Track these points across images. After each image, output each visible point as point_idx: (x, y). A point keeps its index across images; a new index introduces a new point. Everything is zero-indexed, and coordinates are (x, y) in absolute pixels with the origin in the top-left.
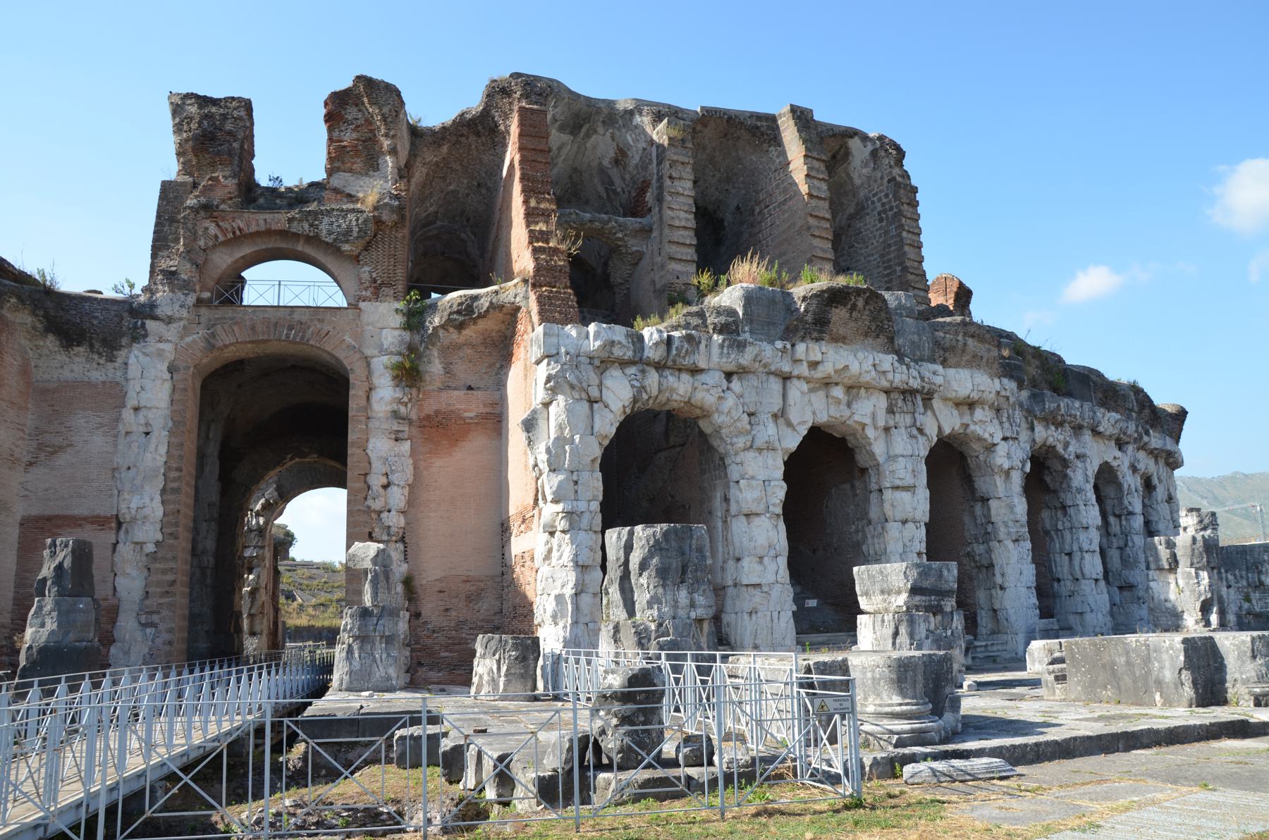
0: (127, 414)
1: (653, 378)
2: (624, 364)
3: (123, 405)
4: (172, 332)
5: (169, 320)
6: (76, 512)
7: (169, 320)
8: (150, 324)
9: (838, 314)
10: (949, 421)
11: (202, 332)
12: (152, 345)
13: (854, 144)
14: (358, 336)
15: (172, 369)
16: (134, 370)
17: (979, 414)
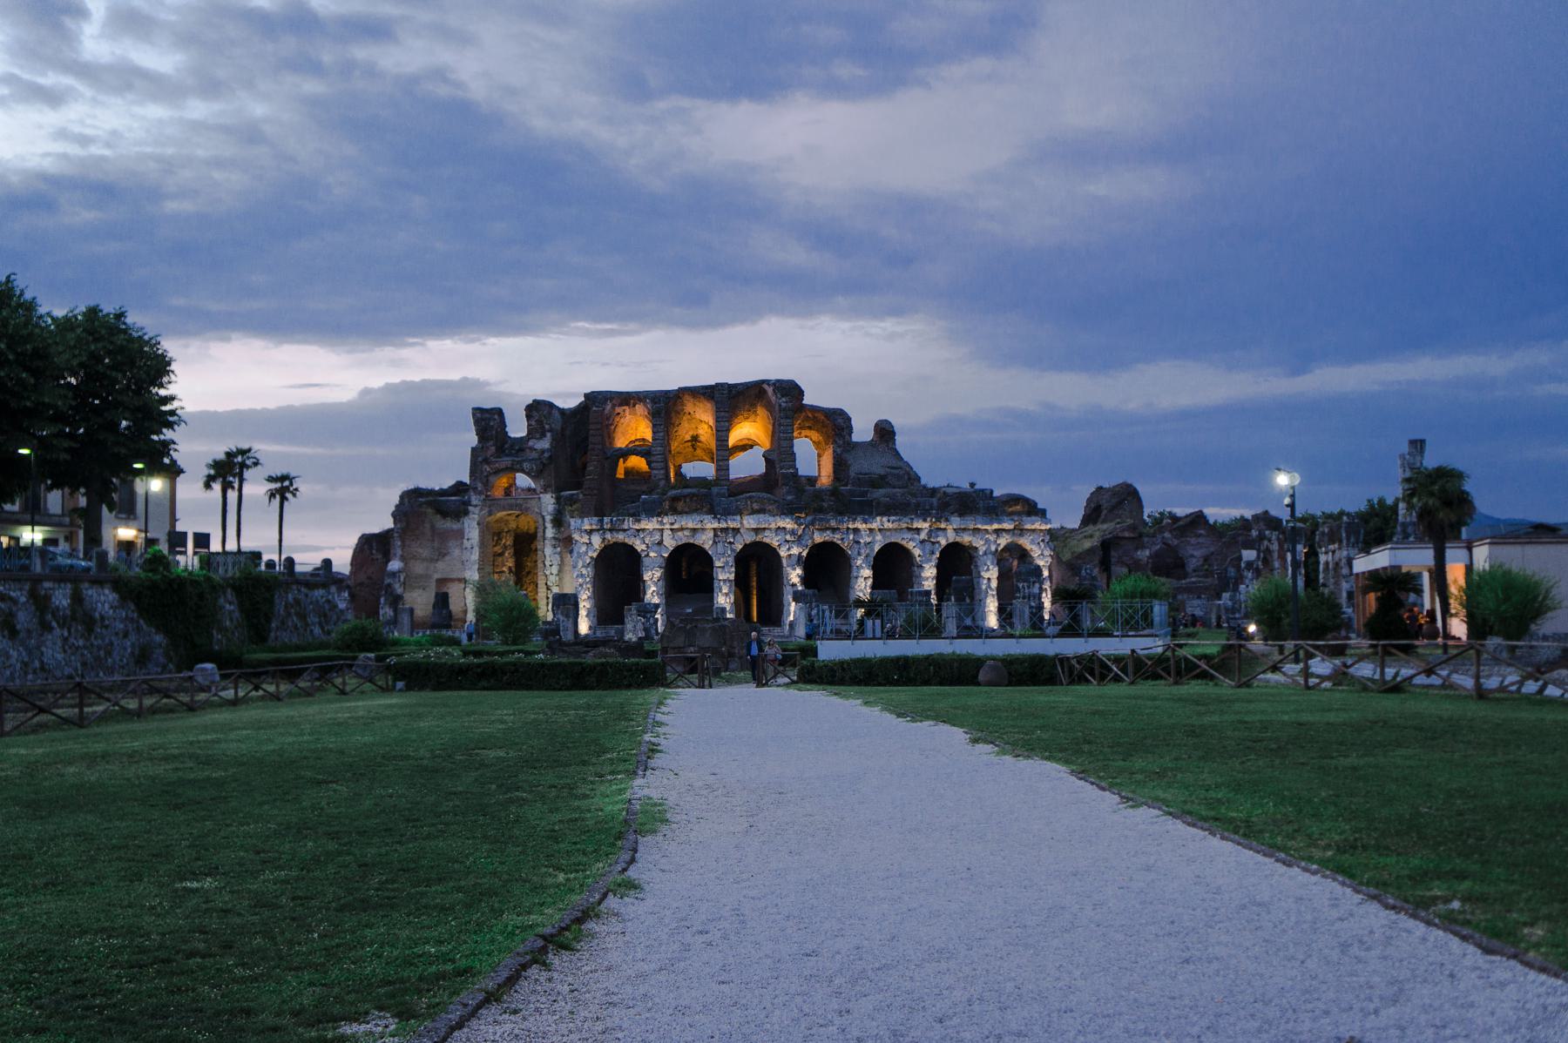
0: (465, 541)
1: (608, 536)
2: (598, 530)
3: (463, 538)
4: (477, 510)
5: (476, 506)
6: (454, 576)
7: (476, 506)
8: (470, 508)
9: (680, 505)
10: (749, 538)
11: (487, 509)
12: (471, 516)
13: (765, 386)
14: (540, 508)
15: (478, 524)
16: (466, 525)
17: (767, 533)
